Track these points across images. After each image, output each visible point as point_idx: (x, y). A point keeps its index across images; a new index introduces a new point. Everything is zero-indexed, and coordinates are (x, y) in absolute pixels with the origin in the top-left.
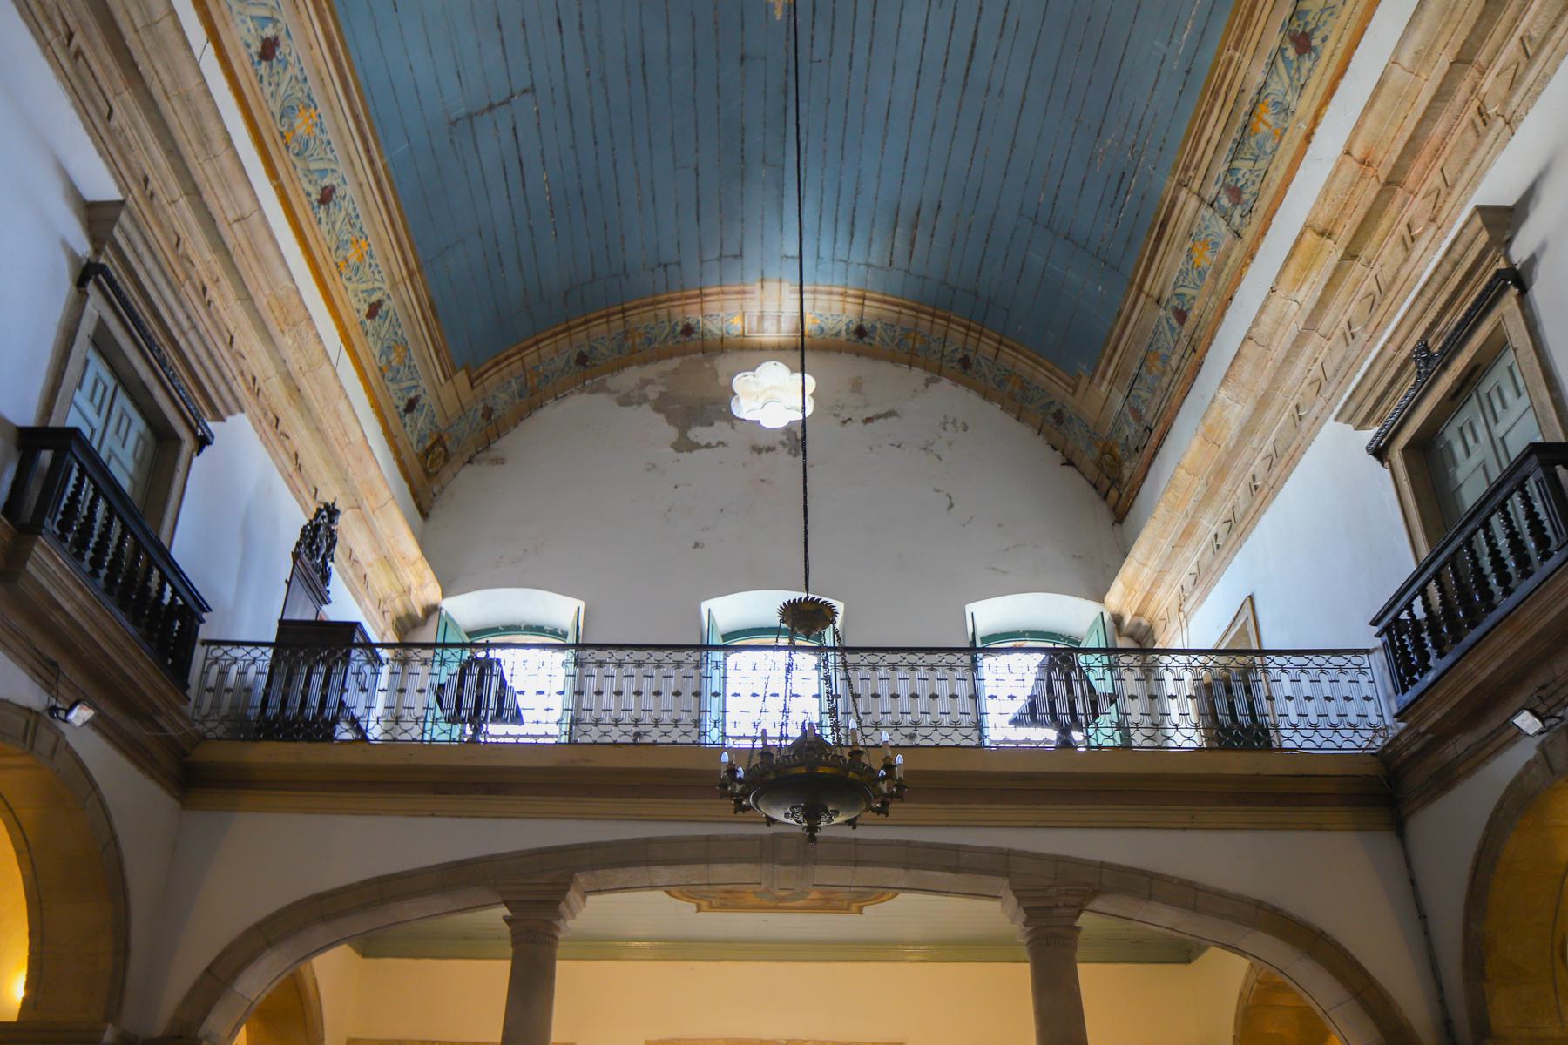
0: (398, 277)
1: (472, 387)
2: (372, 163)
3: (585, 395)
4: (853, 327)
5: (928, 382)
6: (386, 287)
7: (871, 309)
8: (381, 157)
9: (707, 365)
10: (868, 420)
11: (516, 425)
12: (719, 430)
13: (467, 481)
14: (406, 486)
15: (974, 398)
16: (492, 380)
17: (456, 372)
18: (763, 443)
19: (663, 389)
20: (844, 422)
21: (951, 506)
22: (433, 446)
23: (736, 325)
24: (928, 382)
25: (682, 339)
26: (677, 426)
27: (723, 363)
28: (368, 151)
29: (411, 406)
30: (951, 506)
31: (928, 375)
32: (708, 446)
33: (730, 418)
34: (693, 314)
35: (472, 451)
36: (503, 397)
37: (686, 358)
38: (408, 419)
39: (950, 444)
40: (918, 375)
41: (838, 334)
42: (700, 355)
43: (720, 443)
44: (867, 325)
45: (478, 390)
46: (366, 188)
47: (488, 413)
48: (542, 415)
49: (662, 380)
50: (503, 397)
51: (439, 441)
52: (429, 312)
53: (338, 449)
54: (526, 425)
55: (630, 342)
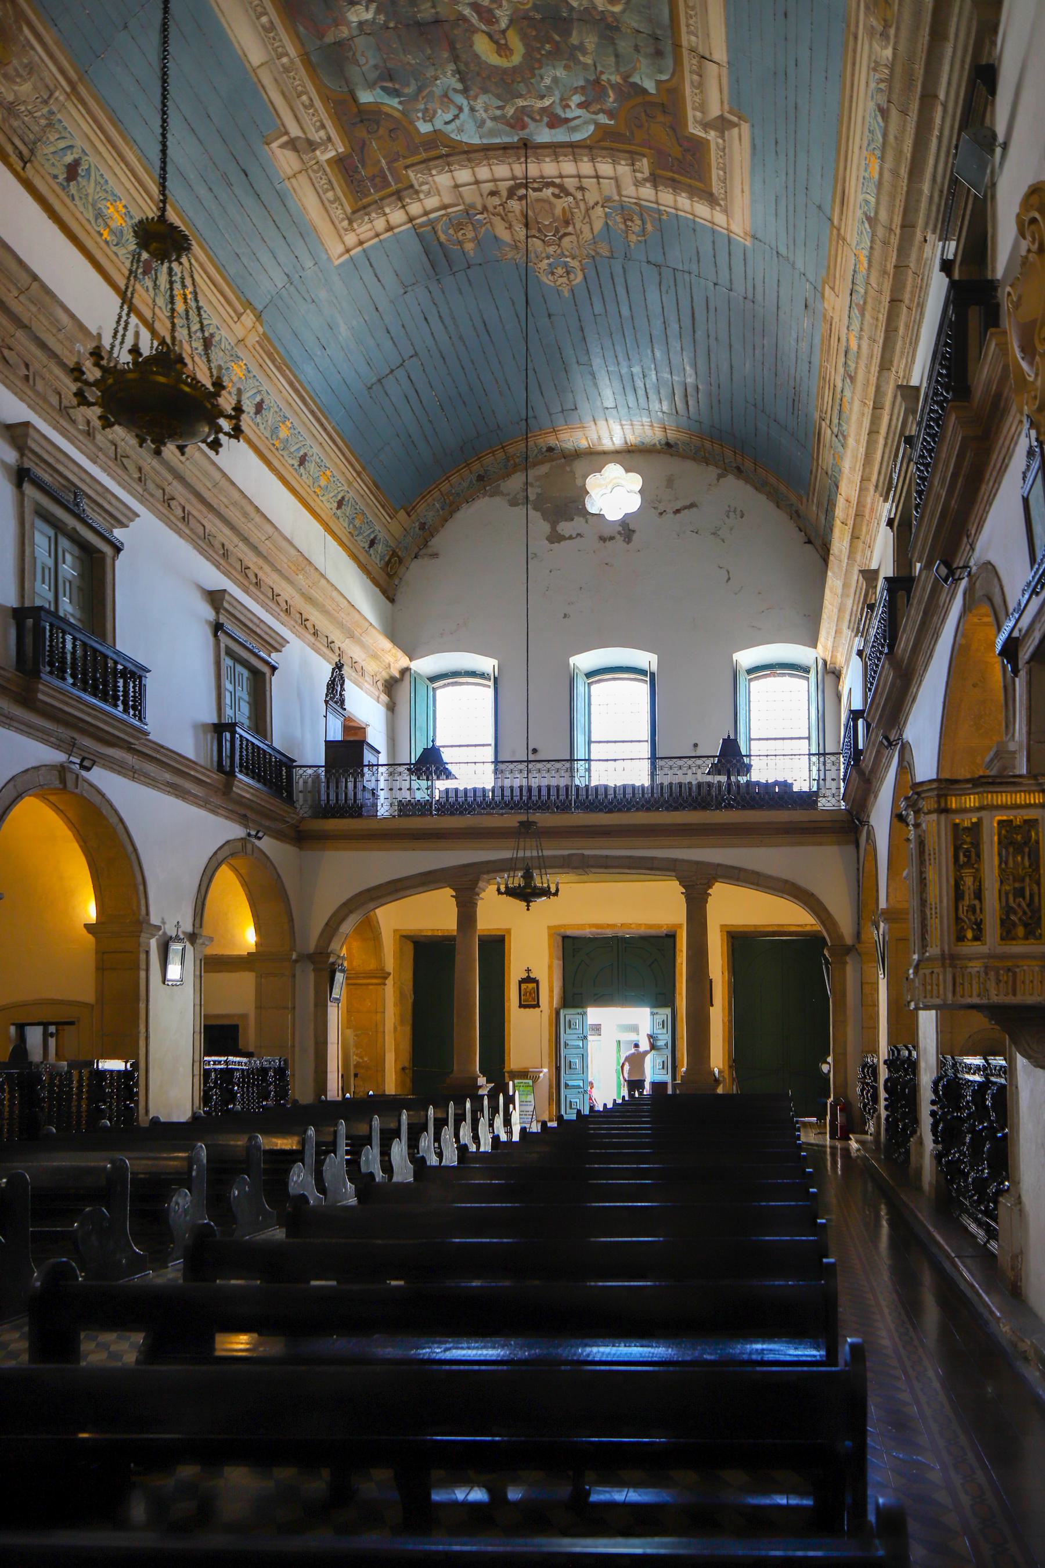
0: (351, 479)
1: (409, 516)
2: (325, 429)
3: (487, 498)
4: (663, 442)
5: (720, 477)
6: (346, 488)
7: (672, 436)
8: (330, 424)
9: (568, 469)
10: (677, 511)
11: (443, 526)
12: (579, 521)
13: (415, 571)
14: (377, 590)
15: (749, 488)
16: (422, 508)
17: (397, 512)
18: (607, 533)
19: (539, 490)
20: (661, 514)
21: (729, 579)
22: (390, 560)
23: (584, 444)
24: (720, 477)
25: (547, 454)
26: (549, 521)
27: (579, 466)
28: (322, 425)
29: (372, 543)
30: (729, 579)
31: (719, 471)
32: (570, 538)
33: (585, 513)
34: (552, 441)
35: (416, 550)
36: (431, 514)
37: (554, 463)
38: (372, 551)
39: (731, 530)
40: (712, 472)
41: (654, 445)
42: (563, 460)
43: (579, 535)
44: (671, 442)
45: (413, 517)
46: (325, 444)
47: (422, 526)
48: (459, 515)
49: (538, 483)
50: (431, 514)
51: (394, 554)
52: (374, 489)
53: (336, 614)
54: (449, 525)
55: (512, 462)
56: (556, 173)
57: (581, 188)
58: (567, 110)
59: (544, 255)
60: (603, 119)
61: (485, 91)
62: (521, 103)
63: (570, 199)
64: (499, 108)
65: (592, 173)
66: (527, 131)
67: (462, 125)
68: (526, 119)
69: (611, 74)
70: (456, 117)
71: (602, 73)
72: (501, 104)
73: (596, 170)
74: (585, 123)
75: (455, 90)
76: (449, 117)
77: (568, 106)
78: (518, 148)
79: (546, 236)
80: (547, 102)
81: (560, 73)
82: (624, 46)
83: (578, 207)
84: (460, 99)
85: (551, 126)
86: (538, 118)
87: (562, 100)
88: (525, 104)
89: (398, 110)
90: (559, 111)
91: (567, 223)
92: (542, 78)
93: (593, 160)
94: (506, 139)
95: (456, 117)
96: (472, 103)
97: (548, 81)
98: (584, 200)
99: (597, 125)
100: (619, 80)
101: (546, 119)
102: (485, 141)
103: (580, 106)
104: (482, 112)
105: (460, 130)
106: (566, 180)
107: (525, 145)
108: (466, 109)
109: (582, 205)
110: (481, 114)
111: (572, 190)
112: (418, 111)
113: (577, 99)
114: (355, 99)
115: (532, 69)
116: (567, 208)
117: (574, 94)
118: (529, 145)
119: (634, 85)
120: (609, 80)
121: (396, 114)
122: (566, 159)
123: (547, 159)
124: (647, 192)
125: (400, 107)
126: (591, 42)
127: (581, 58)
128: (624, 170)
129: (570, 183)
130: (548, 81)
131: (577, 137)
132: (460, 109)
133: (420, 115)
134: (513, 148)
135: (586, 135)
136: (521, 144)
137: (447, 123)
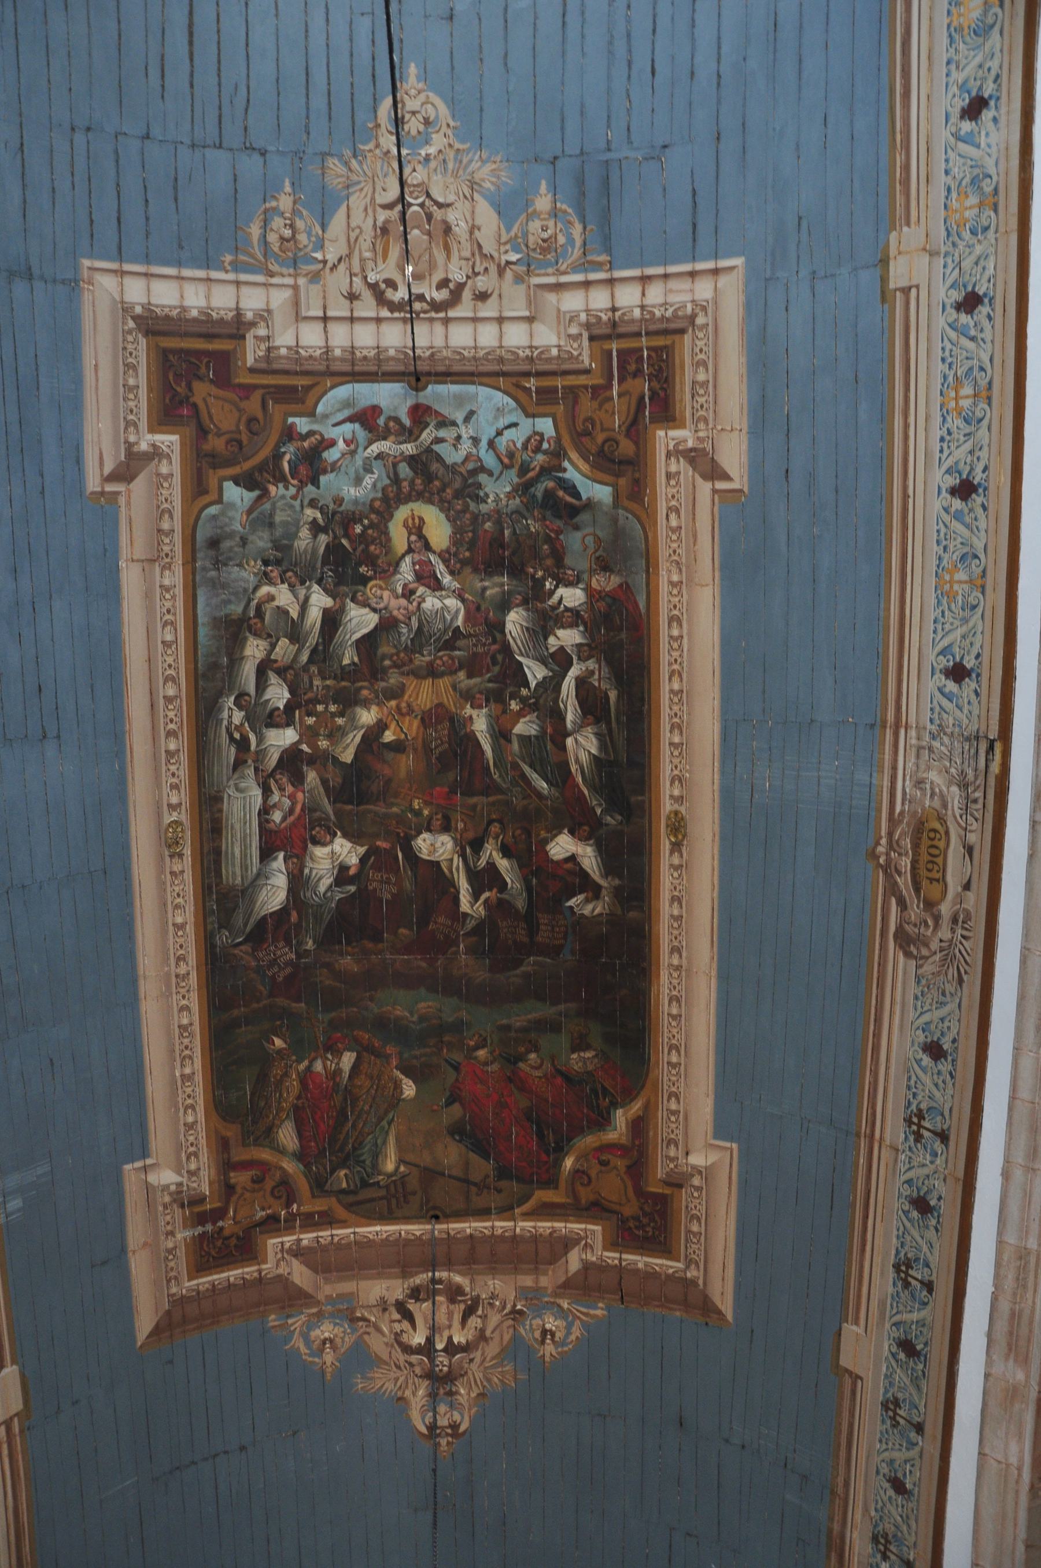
56: (385, 327)
57: (352, 297)
58: (349, 436)
59: (433, 164)
60: (302, 424)
61: (453, 469)
62: (409, 449)
63: (372, 278)
64: (439, 441)
65: (332, 327)
66: (410, 403)
67: (496, 418)
68: (407, 422)
69: (283, 497)
70: (499, 433)
71: (294, 498)
72: (435, 447)
73: (326, 332)
74: (326, 416)
75: (490, 474)
76: (509, 434)
77: (347, 443)
78: (429, 374)
79: (422, 205)
80: (375, 448)
81: (351, 492)
82: (261, 541)
83: (362, 260)
84: (489, 460)
85: (375, 410)
86: (392, 424)
87: (353, 453)
88: (403, 447)
89: (570, 460)
90: (361, 434)
91: (385, 230)
92: (374, 485)
93: (328, 349)
94: (441, 389)
95: (499, 433)
96: (474, 451)
97: (368, 480)
98: (352, 275)
99: (312, 414)
100: (272, 489)
101: (381, 421)
102: (471, 388)
103: (333, 443)
104: (465, 436)
105: (500, 411)
106: (372, 314)
107: (418, 380)
108: (484, 443)
109: (356, 269)
110: (466, 432)
111: (367, 295)
112: (545, 452)
113: (332, 455)
114: (616, 496)
115: (385, 499)
116: (380, 261)
117: (336, 462)
118: (413, 380)
119: (249, 489)
120: (287, 488)
121: (574, 455)
122: (365, 352)
123: (392, 352)
124: (252, 301)
125: (566, 464)
126: (304, 539)
127: (319, 515)
128: (284, 340)
129: (367, 307)
130: (368, 480)
131: (343, 392)
132: (491, 444)
133: (545, 446)
134: (437, 374)
135: (331, 394)
136: (423, 379)
137: (515, 425)
